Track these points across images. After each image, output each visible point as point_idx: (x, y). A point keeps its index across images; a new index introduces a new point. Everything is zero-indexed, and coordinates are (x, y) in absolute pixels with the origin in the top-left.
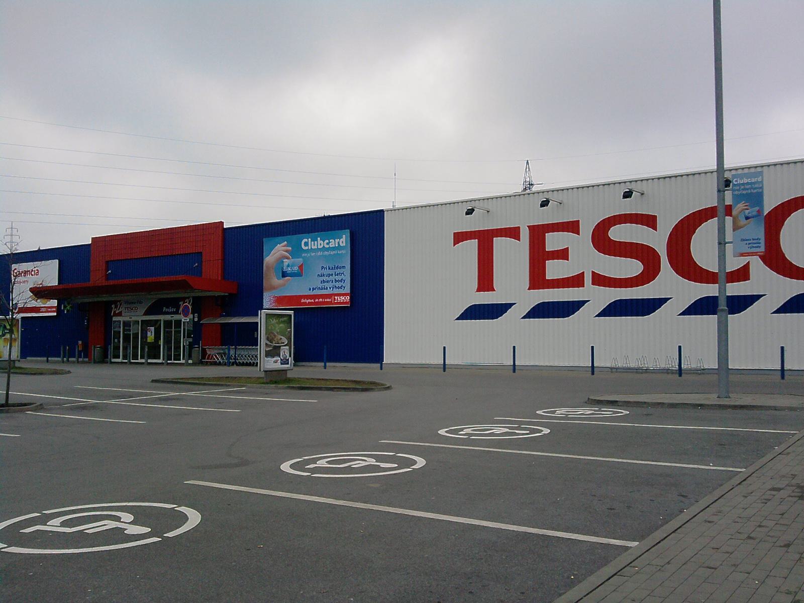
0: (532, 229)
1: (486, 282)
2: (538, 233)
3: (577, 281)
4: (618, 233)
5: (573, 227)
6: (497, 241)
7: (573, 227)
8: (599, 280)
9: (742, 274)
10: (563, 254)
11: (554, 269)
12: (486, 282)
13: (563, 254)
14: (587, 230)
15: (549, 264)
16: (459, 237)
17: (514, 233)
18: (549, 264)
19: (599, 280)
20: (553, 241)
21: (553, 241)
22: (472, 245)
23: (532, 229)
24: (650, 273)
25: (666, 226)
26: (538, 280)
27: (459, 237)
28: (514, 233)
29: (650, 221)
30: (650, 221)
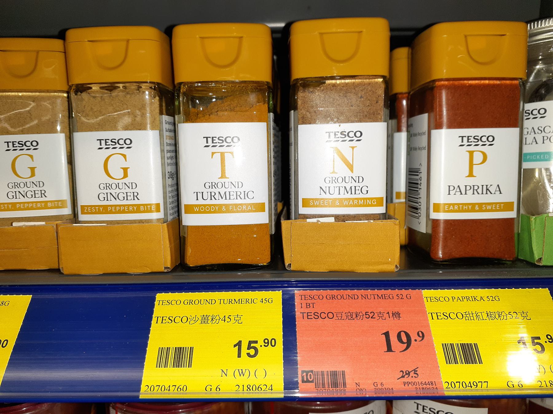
0: (212, 137)
1: (207, 143)
2: (213, 138)
4: (220, 138)
5: (216, 137)
6: (208, 138)
7: (216, 137)
8: (218, 143)
10: (215, 140)
11: (214, 141)
13: (215, 140)
14: (217, 138)
16: (204, 137)
17: (210, 137)
19: (218, 143)
20: (214, 139)
21: (214, 139)
23: (212, 137)
25: (224, 138)
26: (213, 143)
27: (204, 137)
28: (210, 137)
29: (223, 137)
30: (223, 137)
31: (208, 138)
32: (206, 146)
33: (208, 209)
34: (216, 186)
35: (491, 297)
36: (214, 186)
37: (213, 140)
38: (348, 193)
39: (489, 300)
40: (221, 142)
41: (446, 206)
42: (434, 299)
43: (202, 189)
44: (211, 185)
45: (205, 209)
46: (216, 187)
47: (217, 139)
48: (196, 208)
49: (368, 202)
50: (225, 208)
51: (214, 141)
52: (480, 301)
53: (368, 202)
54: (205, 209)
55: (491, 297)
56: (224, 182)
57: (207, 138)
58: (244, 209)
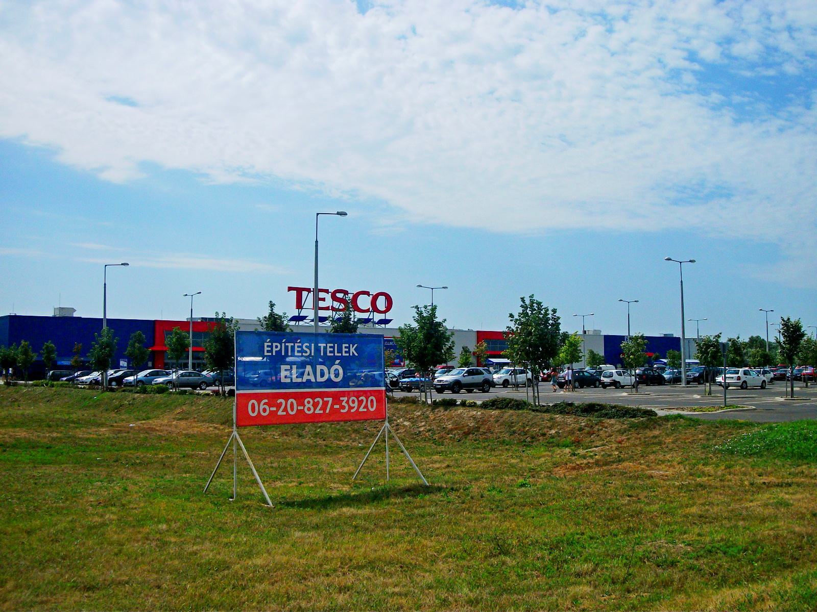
3: (327, 308)
4: (340, 295)
5: (327, 291)
7: (327, 291)
8: (333, 309)
9: (367, 311)
10: (323, 299)
11: (321, 304)
12: (299, 306)
13: (323, 299)
16: (290, 289)
19: (333, 309)
20: (322, 295)
21: (322, 295)
22: (295, 292)
27: (290, 289)
31: (305, 294)
37: (317, 299)
47: (328, 297)
51: (321, 304)
57: (299, 291)
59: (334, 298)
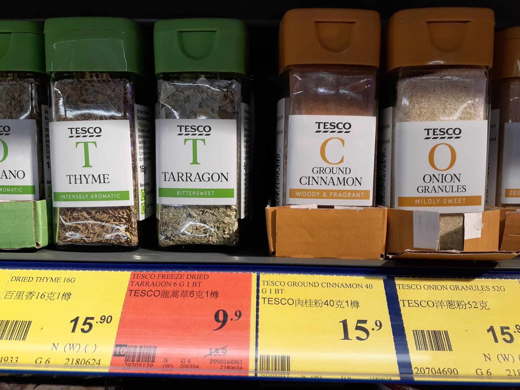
1: (319, 128)
3: (328, 128)
5: (328, 123)
6: (321, 124)
8: (330, 128)
10: (327, 126)
13: (327, 126)
14: (329, 123)
15: (326, 126)
17: (322, 123)
18: (326, 126)
20: (326, 124)
21: (326, 124)
22: (318, 124)
23: (324, 123)
24: (334, 128)
26: (324, 128)
28: (322, 123)
29: (335, 123)
30: (335, 123)
31: (321, 124)
32: (317, 132)
33: (309, 194)
34: (324, 171)
35: (496, 287)
36: (322, 171)
37: (325, 126)
38: (341, 184)
39: (494, 290)
40: (333, 127)
41: (455, 199)
42: (406, 286)
43: (311, 175)
44: (319, 170)
45: (306, 194)
46: (324, 172)
47: (329, 125)
48: (298, 193)
49: (359, 194)
50: (325, 194)
52: (462, 290)
53: (359, 194)
54: (306, 194)
55: (496, 287)
56: (333, 168)
58: (349, 195)
59: (330, 124)
